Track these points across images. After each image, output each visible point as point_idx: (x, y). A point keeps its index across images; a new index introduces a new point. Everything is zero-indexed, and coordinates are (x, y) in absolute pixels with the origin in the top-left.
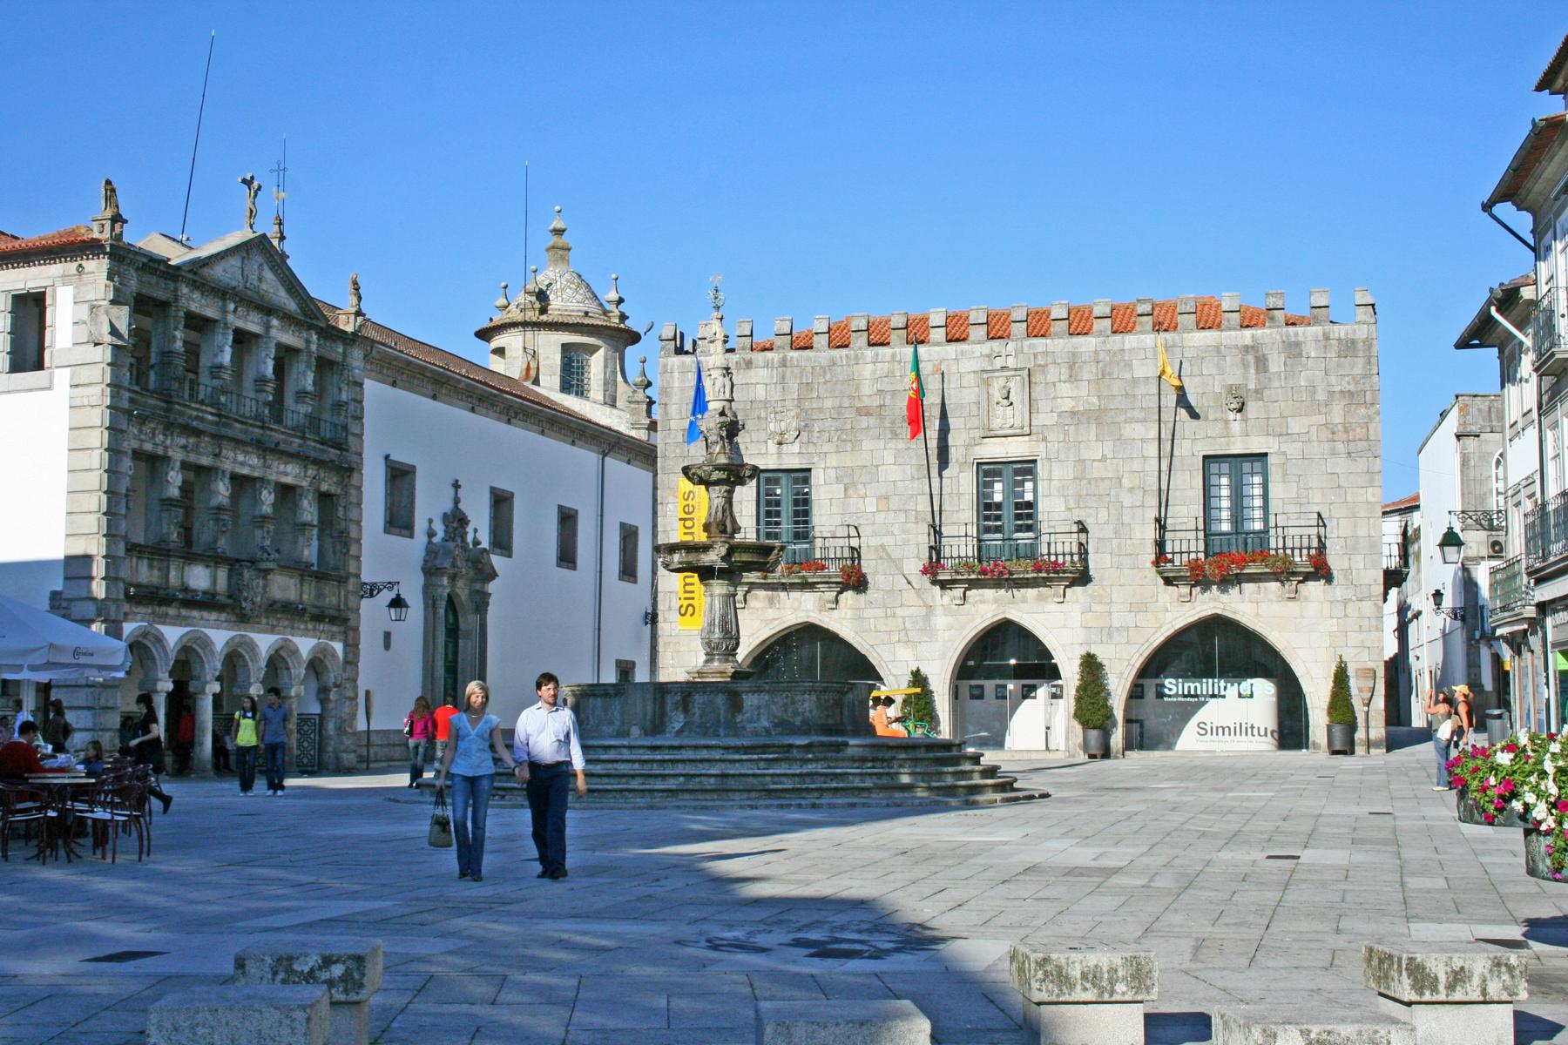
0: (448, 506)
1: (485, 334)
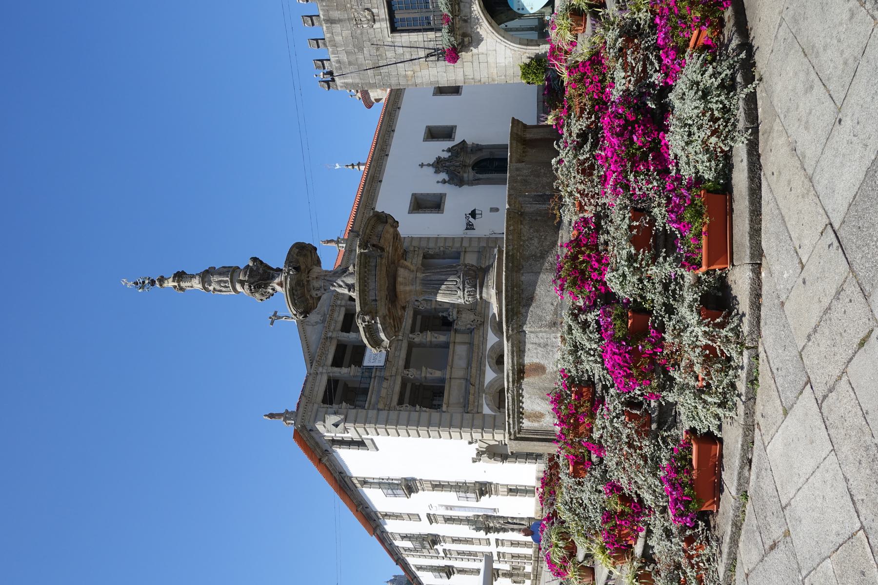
0: (431, 170)
1: (369, 104)
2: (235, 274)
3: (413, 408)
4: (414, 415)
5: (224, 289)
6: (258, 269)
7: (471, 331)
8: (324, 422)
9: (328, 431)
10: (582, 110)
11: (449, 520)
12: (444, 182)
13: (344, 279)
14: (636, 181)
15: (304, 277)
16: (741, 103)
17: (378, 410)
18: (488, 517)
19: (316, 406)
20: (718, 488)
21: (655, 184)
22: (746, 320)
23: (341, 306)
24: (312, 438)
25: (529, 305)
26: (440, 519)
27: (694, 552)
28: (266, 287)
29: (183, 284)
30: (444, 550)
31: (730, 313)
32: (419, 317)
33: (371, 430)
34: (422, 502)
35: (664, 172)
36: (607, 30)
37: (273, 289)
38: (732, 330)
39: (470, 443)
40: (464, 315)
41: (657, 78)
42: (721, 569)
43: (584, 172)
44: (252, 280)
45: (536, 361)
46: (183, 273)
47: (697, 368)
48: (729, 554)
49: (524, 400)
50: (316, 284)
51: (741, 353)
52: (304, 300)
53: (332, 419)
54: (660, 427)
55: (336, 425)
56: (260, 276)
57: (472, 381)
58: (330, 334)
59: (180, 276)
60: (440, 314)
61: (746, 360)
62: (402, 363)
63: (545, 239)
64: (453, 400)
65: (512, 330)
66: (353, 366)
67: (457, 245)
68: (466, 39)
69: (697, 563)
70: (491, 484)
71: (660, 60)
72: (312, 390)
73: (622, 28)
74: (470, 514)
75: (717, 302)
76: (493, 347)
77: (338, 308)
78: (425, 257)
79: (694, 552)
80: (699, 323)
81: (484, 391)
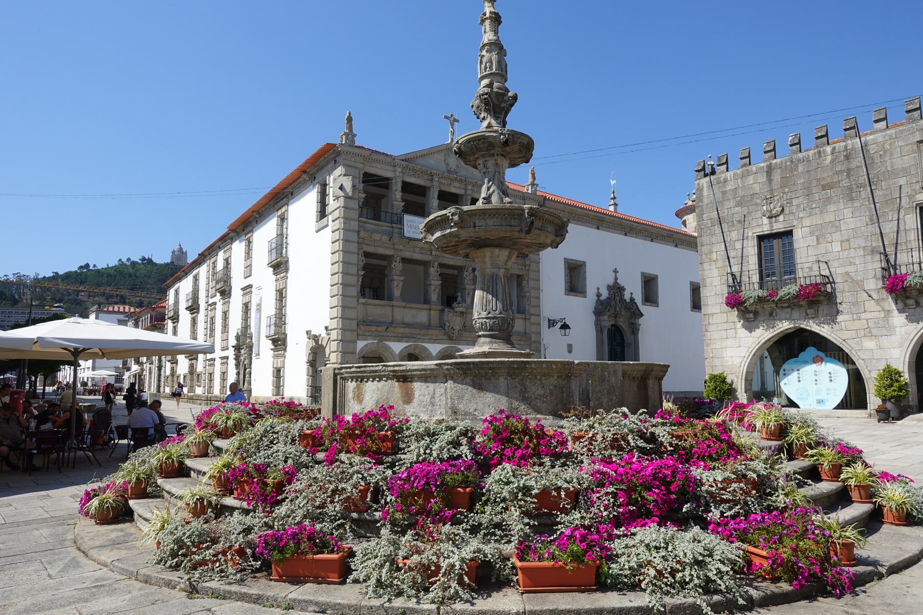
0: (611, 281)
1: (680, 214)
2: (499, 78)
3: (360, 268)
4: (354, 269)
5: (483, 66)
6: (505, 102)
7: (442, 326)
8: (345, 175)
9: (335, 180)
10: (679, 438)
11: (246, 307)
12: (599, 295)
13: (496, 193)
14: (607, 494)
15: (498, 150)
16: (690, 600)
17: (359, 232)
18: (250, 348)
19: (361, 166)
20: (296, 580)
21: (605, 514)
22: (467, 606)
23: (466, 189)
24: (327, 164)
25: (474, 386)
26: (247, 299)
27: (229, 557)
28: (487, 110)
29: (487, 22)
30: (215, 303)
31: (473, 590)
32: (455, 272)
33: (337, 224)
34: (264, 279)
35: (617, 522)
36: (765, 461)
37: (484, 119)
38: (457, 592)
39: (326, 328)
40: (458, 319)
41: (715, 514)
42: (214, 584)
43: (615, 440)
44: (493, 96)
45: (417, 394)
46: (500, 23)
47: (416, 558)
48: (230, 592)
49: (375, 382)
50: (490, 163)
51: (433, 602)
52: (474, 151)
53: (348, 183)
54: (353, 521)
55: (341, 188)
56: (498, 104)
57: (391, 329)
58: (436, 179)
59: (496, 19)
60: (459, 294)
61: (426, 607)
62: (408, 255)
63: (544, 402)
64: (370, 309)
65: (447, 369)
66: (403, 204)
67: (532, 311)
68: (751, 315)
69: (219, 560)
70: (285, 350)
71: (734, 517)
72: (377, 161)
73: (768, 477)
74: (253, 329)
75: (485, 578)
76: (426, 349)
77: (463, 186)
78: (519, 276)
79: (229, 557)
80: (463, 560)
81: (380, 341)
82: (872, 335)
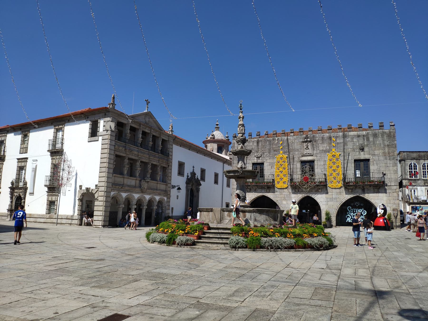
0: (192, 171)
12: (188, 176)
23: (151, 131)
40: (147, 184)
62: (131, 156)
82: (285, 199)
